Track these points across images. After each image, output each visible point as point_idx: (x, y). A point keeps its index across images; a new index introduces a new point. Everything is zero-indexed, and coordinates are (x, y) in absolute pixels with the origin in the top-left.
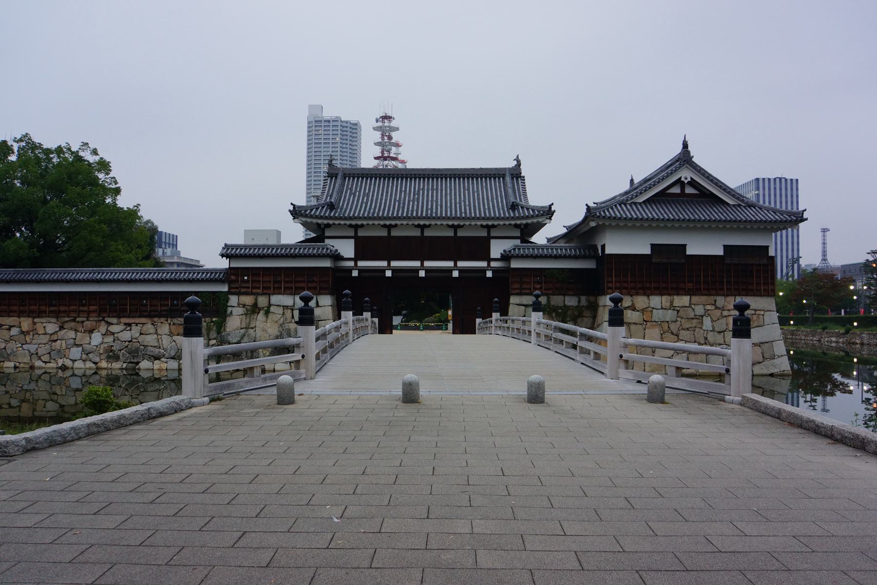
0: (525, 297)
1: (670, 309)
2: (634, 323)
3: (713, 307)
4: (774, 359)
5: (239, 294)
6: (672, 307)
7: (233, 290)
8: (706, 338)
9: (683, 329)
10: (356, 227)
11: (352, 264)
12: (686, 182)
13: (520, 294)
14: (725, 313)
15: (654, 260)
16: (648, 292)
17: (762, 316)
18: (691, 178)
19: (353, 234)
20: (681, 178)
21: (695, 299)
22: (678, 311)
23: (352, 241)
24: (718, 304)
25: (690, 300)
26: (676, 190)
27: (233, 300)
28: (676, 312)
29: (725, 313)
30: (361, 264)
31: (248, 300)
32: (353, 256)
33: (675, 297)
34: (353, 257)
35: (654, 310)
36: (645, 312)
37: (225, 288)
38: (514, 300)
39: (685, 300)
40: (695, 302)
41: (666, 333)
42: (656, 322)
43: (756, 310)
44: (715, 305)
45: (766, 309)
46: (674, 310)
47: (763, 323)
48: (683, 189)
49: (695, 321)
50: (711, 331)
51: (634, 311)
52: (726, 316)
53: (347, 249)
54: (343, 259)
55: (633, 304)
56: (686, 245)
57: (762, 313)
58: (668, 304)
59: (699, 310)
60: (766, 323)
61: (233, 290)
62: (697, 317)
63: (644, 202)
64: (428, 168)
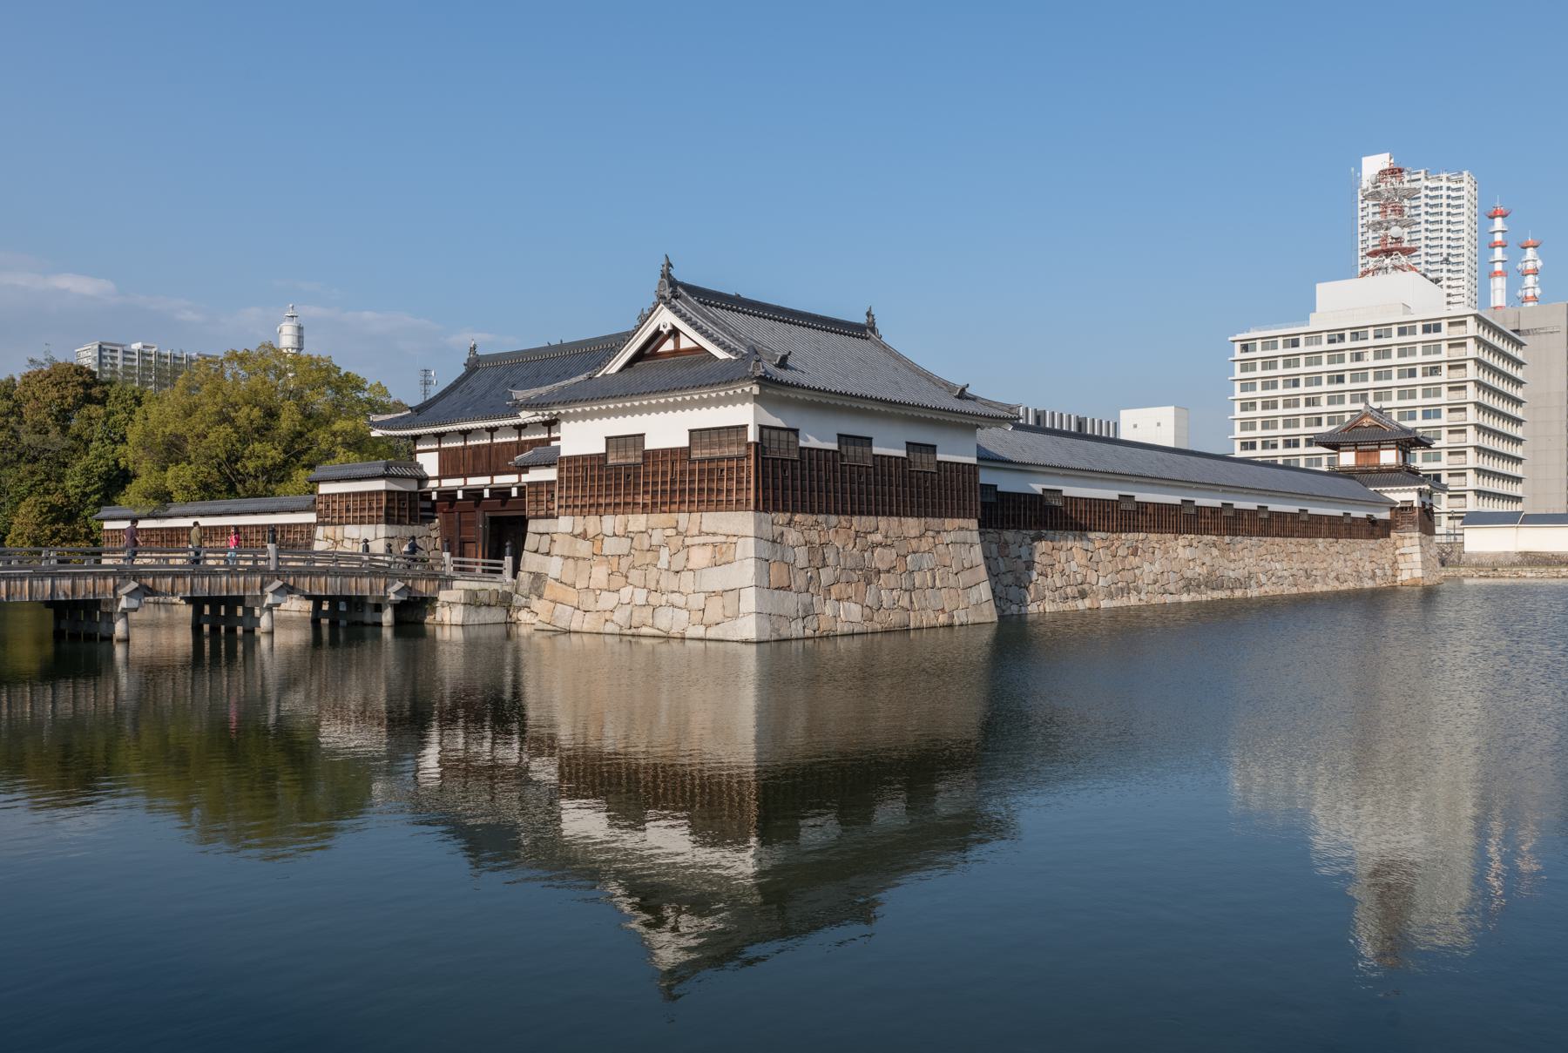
0: (541, 520)
1: (624, 536)
2: (584, 559)
3: (673, 532)
4: (737, 617)
5: (324, 524)
6: (627, 534)
7: (320, 520)
8: (658, 582)
9: (634, 567)
10: (440, 436)
11: (433, 484)
12: (665, 331)
13: (537, 517)
14: (688, 541)
15: (610, 462)
16: (597, 509)
17: (733, 545)
18: (671, 324)
19: (437, 446)
20: (659, 326)
21: (658, 519)
22: (632, 539)
23: (437, 453)
24: (681, 529)
25: (647, 521)
26: (669, 346)
27: (320, 532)
28: (629, 540)
29: (688, 541)
30: (448, 483)
31: (329, 530)
32: (437, 474)
33: (630, 517)
34: (437, 474)
35: (606, 538)
36: (596, 542)
37: (311, 518)
38: (533, 526)
39: (638, 521)
40: (653, 526)
41: (615, 574)
42: (607, 556)
43: (728, 536)
44: (676, 528)
45: (740, 534)
46: (628, 537)
47: (732, 558)
48: (677, 343)
49: (650, 555)
50: (666, 570)
51: (584, 539)
52: (688, 546)
53: (429, 463)
54: (428, 479)
55: (585, 530)
56: (642, 435)
57: (735, 539)
58: (622, 529)
59: (657, 537)
60: (737, 557)
61: (320, 520)
62: (654, 548)
63: (621, 370)
64: (555, 342)
